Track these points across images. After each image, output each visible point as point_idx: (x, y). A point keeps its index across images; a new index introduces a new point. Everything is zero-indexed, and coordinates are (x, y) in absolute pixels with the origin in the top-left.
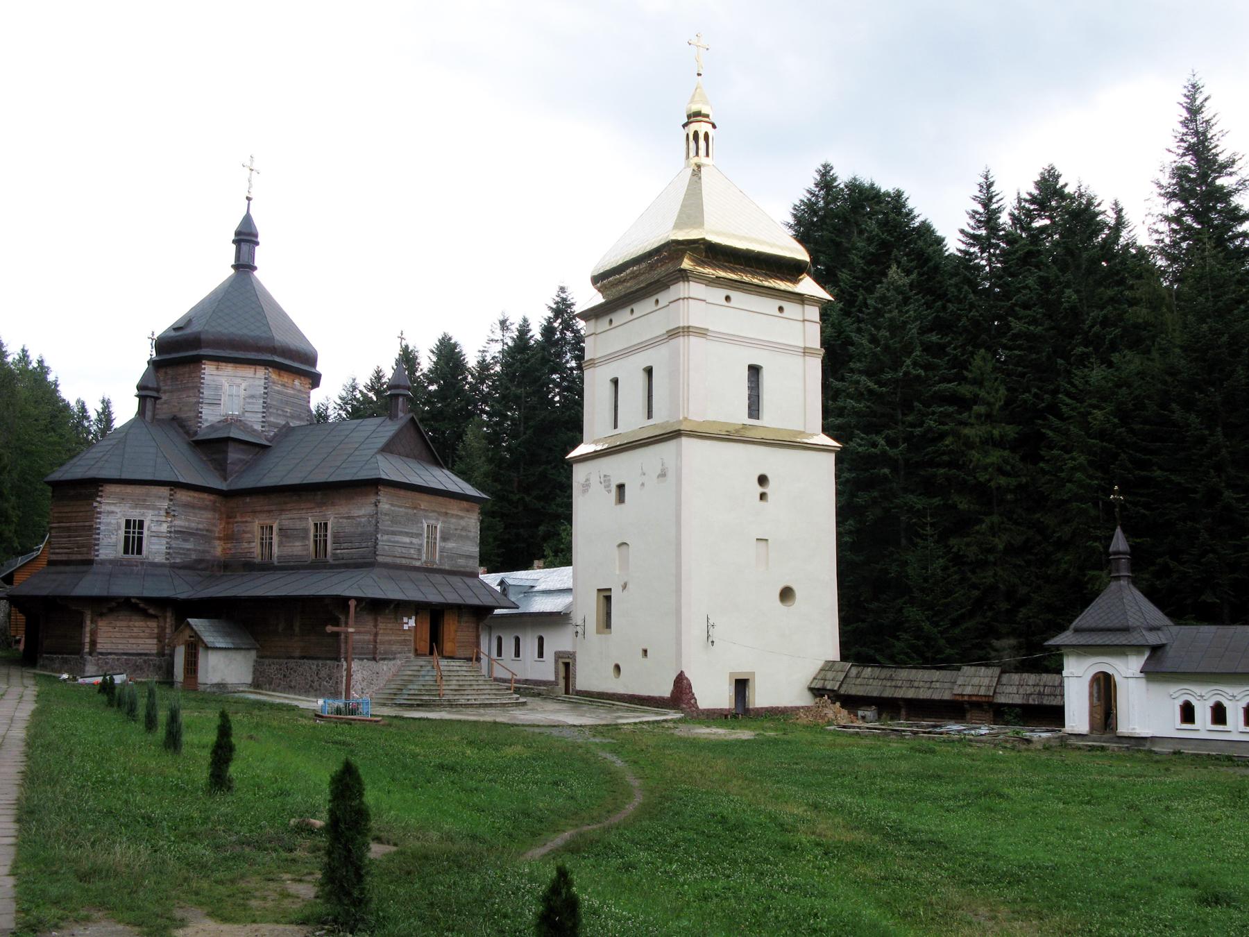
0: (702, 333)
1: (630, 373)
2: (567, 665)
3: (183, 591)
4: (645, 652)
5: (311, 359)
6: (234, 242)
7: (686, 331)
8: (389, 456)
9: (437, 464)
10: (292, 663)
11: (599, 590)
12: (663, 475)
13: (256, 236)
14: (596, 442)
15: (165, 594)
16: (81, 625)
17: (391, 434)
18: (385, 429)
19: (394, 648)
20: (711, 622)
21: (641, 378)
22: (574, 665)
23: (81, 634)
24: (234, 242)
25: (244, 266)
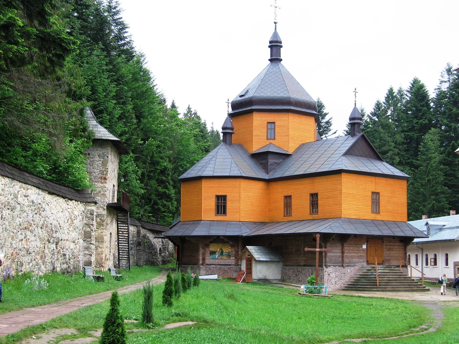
3: (245, 232)
6: (269, 47)
8: (350, 158)
10: (300, 269)
13: (281, 43)
15: (236, 234)
16: (198, 250)
17: (350, 145)
19: (354, 260)
23: (198, 255)
24: (269, 47)
25: (275, 59)
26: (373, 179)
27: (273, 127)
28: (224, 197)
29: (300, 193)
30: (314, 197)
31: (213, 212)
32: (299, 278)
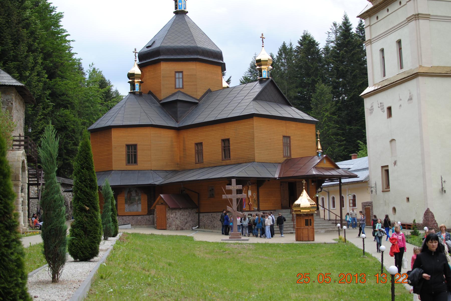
0: (427, 17)
1: (389, 44)
2: (368, 208)
3: (158, 180)
4: (408, 199)
5: (219, 55)
7: (417, 17)
9: (289, 105)
11: (382, 167)
12: (410, 99)
14: (374, 85)
18: (257, 88)
20: (443, 180)
21: (395, 47)
22: (372, 209)
26: (283, 122)
27: (181, 76)
28: (135, 146)
29: (212, 140)
30: (226, 142)
31: (124, 162)
32: (214, 224)
